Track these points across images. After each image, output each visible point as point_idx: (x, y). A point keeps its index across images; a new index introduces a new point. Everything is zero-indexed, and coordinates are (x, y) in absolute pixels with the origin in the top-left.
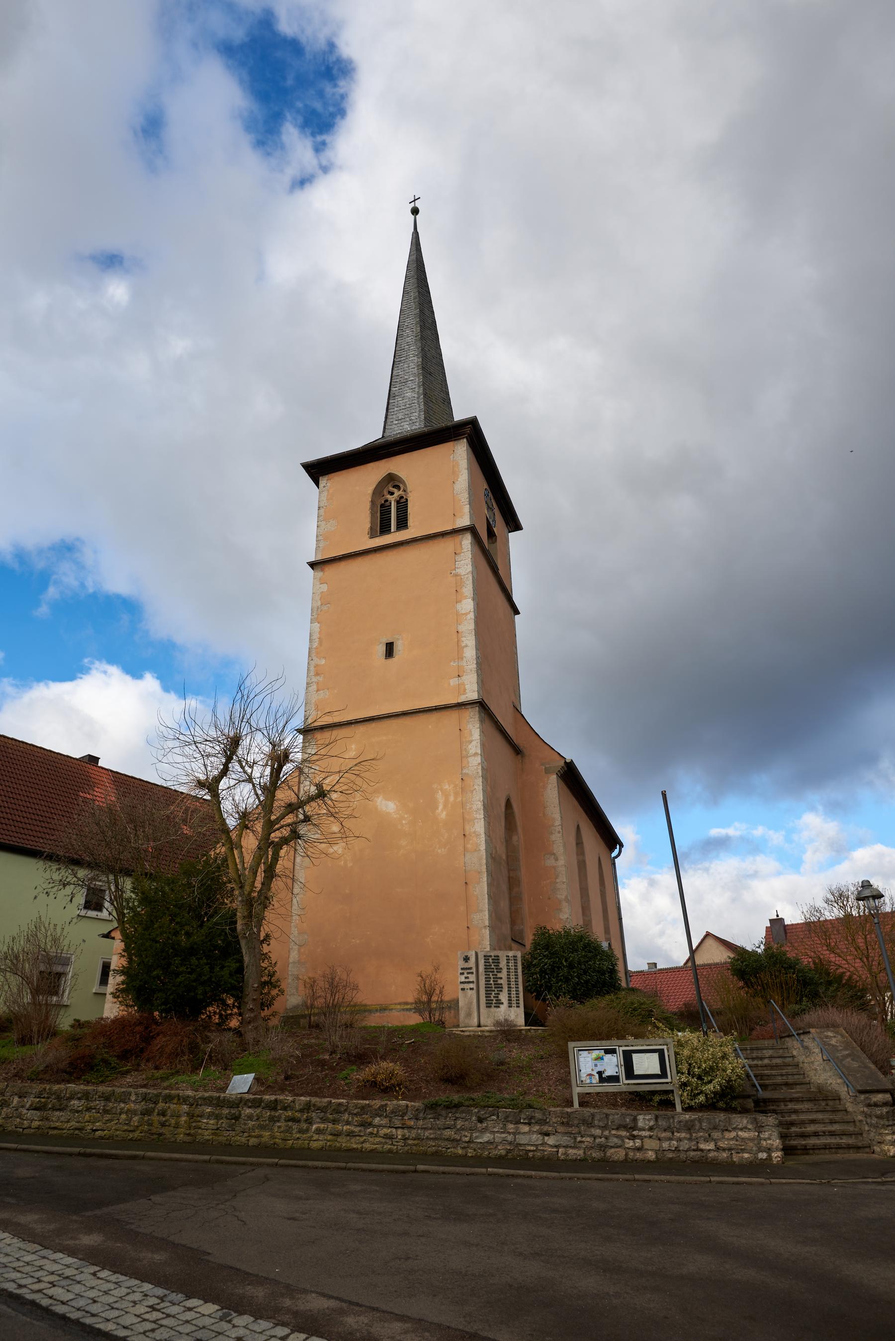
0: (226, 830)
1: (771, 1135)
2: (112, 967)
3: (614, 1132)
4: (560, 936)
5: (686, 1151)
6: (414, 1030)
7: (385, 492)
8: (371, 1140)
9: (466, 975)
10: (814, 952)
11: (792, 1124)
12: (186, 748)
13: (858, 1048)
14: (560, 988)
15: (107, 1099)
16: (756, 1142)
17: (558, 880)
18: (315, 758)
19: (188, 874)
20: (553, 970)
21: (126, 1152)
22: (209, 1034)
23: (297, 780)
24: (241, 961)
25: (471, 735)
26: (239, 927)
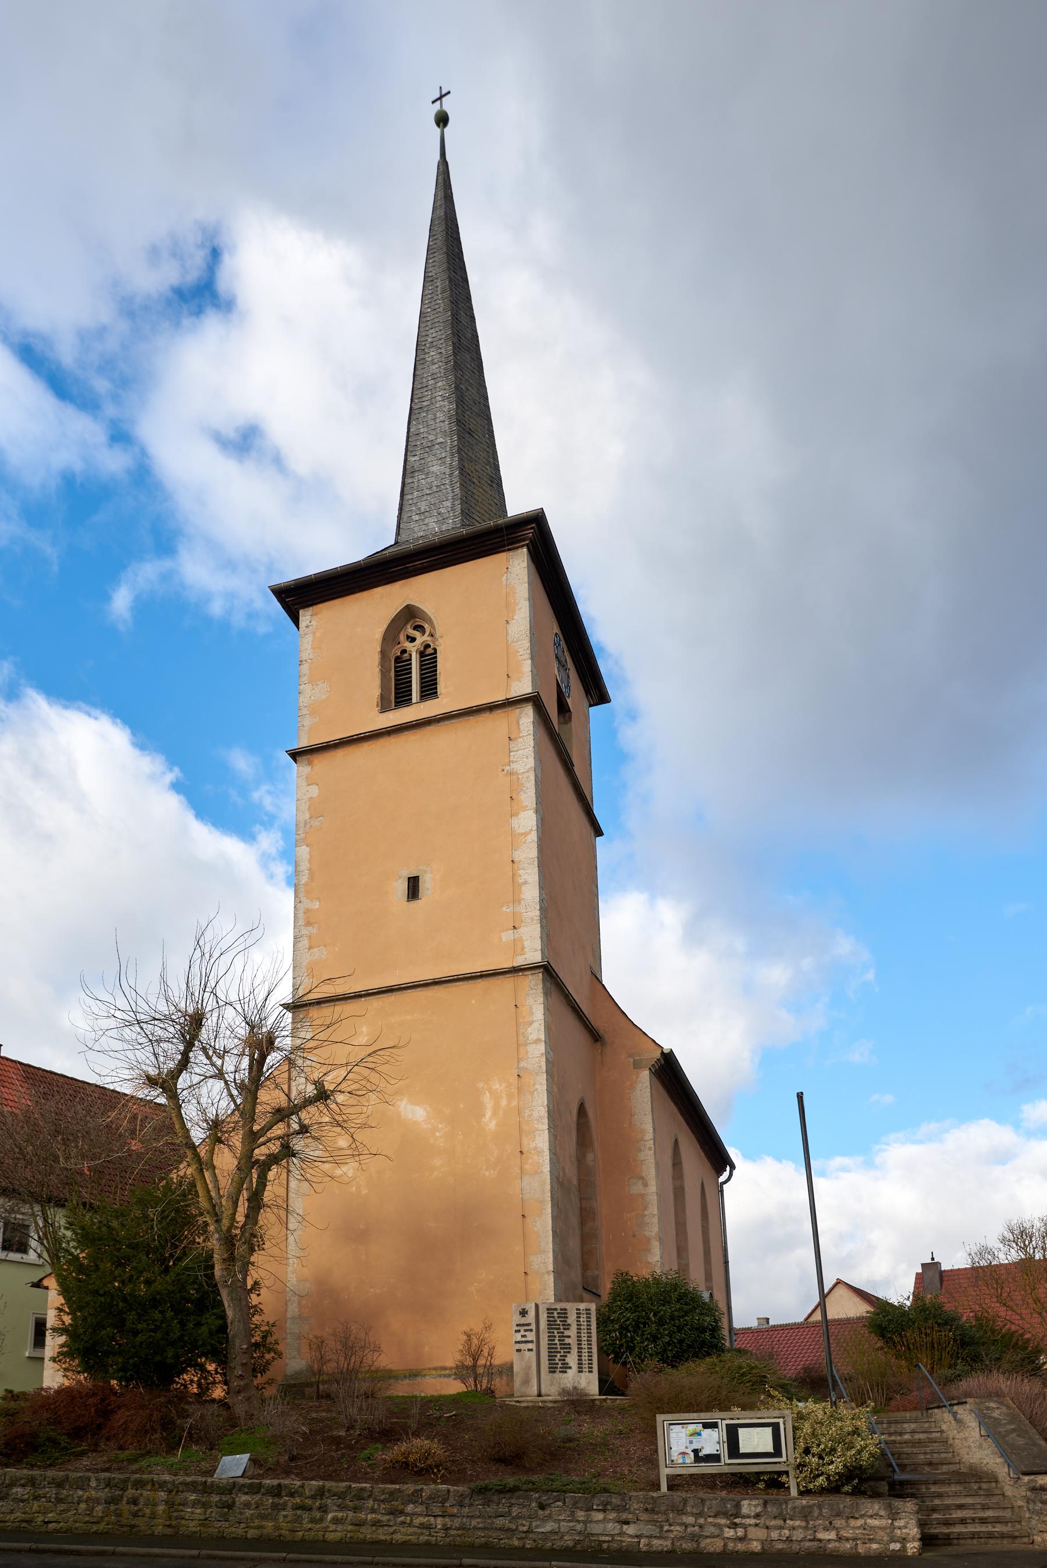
0: (193, 1147)
1: (907, 1523)
2: (49, 1325)
3: (710, 1520)
4: (647, 1284)
5: (801, 1541)
6: (455, 1400)
7: (402, 637)
8: (402, 1530)
9: (522, 1333)
10: (980, 1305)
11: (934, 1510)
12: (127, 1029)
13: (1027, 1422)
14: (646, 1349)
15: (60, 1485)
16: (888, 1531)
17: (646, 1213)
18: (312, 1044)
19: (143, 1204)
20: (637, 1327)
21: (90, 1547)
22: (187, 1407)
23: (286, 1075)
24: (223, 1316)
25: (531, 1013)
26: (218, 1271)
